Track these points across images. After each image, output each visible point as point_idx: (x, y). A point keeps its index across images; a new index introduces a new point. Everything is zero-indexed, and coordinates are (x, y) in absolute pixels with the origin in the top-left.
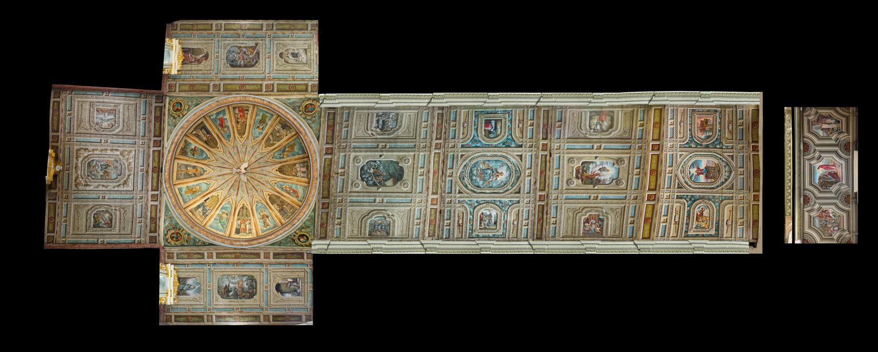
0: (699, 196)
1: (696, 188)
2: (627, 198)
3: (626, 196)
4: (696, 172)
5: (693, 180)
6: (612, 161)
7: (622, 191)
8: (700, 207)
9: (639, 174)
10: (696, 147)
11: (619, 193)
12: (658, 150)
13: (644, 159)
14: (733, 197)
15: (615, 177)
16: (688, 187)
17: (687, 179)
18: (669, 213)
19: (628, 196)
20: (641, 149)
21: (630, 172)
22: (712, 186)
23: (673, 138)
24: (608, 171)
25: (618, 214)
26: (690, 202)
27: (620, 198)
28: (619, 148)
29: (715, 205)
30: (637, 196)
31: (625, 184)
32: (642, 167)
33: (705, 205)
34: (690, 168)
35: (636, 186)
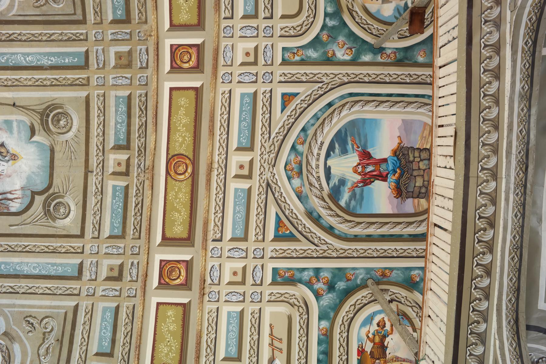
0: (368, 270)
1: (356, 239)
2: (86, 275)
3: (81, 265)
4: (355, 171)
5: (342, 203)
6: (26, 119)
7: (67, 244)
9: (127, 173)
10: (354, 62)
11: (55, 252)
12: (198, 68)
13: (144, 110)
15: (40, 184)
17: (316, 203)
18: (246, 347)
19: (87, 264)
20: (129, 65)
21: (94, 162)
23: (256, 16)
24: (14, 157)
25: (51, 339)
26: (328, 299)
27: (60, 271)
28: (45, 62)
30: (121, 266)
31: (75, 212)
32: (136, 143)
34: (328, 155)
35: (118, 223)
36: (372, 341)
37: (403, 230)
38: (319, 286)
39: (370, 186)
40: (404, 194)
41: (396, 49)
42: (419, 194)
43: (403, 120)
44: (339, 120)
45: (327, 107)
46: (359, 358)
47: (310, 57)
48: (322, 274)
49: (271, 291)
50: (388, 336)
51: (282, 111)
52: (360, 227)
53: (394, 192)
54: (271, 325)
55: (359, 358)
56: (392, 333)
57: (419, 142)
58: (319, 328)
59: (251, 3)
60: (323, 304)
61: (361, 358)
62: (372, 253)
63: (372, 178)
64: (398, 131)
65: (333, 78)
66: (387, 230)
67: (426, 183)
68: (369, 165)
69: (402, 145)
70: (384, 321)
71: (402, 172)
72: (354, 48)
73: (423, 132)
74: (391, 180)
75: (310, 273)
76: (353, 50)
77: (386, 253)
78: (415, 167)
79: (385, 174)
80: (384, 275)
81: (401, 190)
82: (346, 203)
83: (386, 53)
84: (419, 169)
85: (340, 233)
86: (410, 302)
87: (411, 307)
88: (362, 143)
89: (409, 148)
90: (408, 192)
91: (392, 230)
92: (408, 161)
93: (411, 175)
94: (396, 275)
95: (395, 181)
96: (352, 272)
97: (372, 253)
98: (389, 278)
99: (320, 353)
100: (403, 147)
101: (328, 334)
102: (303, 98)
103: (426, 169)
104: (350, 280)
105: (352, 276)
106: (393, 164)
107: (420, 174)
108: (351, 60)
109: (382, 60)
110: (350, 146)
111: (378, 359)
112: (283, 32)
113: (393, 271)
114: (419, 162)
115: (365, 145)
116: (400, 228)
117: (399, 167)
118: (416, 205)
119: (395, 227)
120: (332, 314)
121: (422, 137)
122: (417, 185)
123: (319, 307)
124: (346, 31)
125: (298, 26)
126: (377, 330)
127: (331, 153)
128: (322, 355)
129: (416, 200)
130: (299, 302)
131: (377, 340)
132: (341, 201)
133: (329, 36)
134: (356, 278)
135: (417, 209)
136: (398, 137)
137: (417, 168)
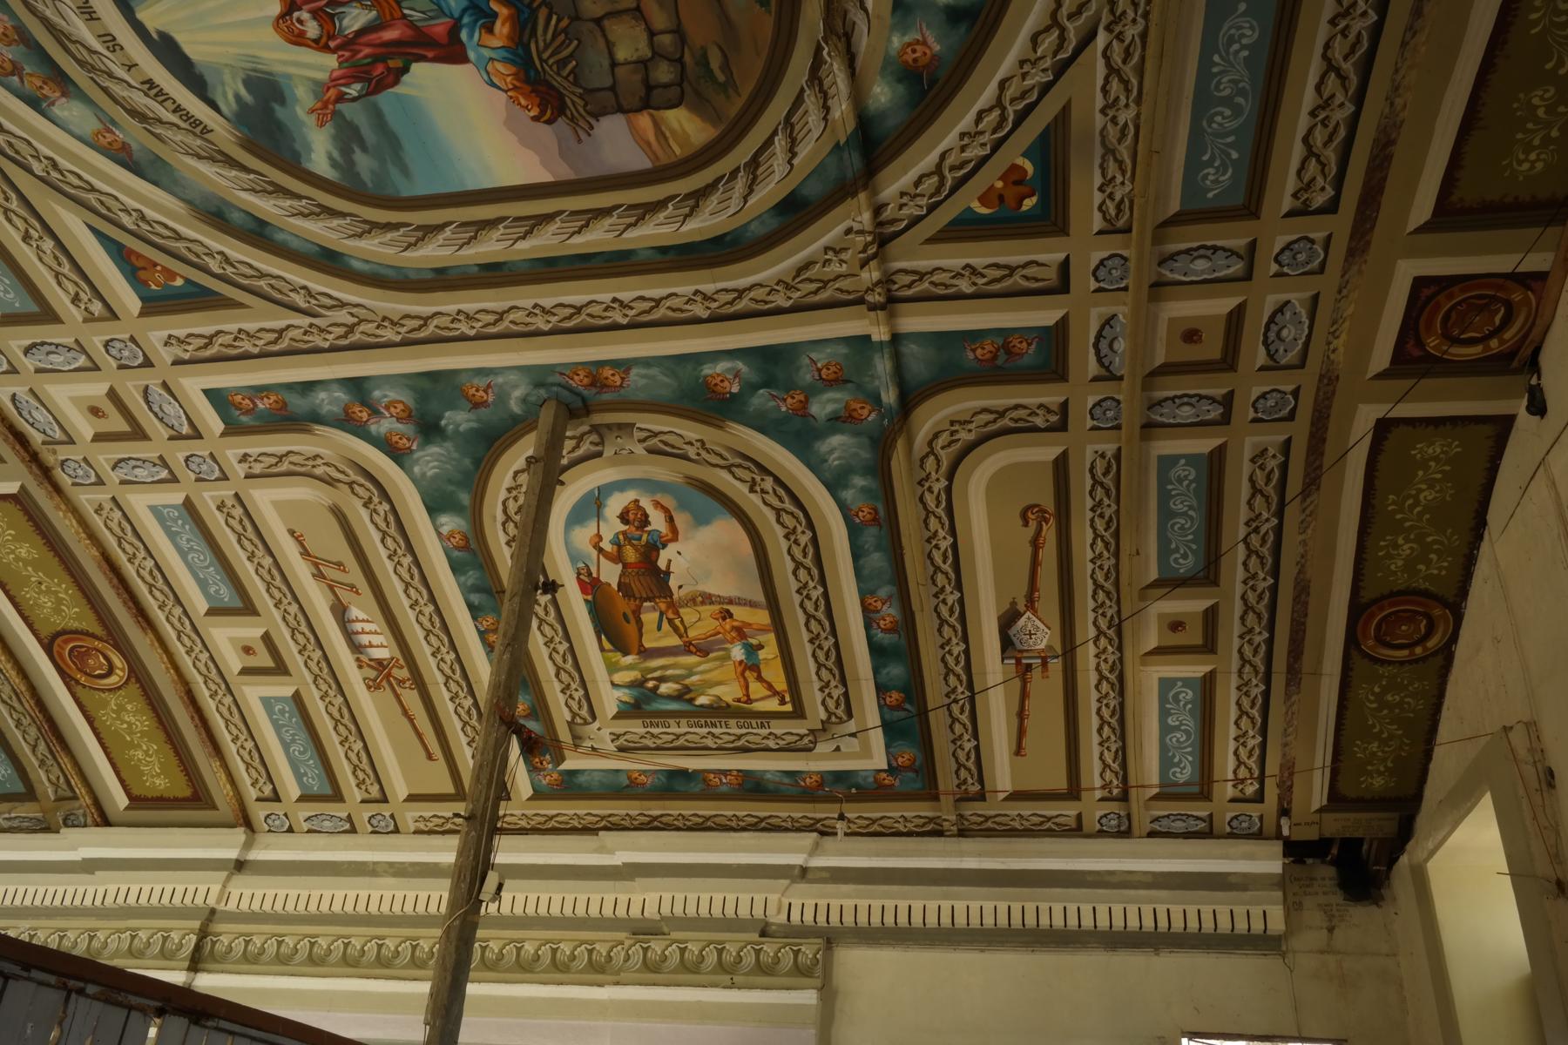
8: (592, 505)
14: (1056, 338)
16: (318, 283)
22: (705, 224)
29: (815, 466)
33: (663, 471)
36: (617, 558)
37: (624, 235)
38: (385, 426)
39: (398, 89)
40: (573, 99)
46: (590, 598)
48: (377, 394)
49: (243, 451)
50: (664, 546)
52: (441, 242)
53: (523, 102)
54: (292, 532)
55: (590, 598)
56: (675, 538)
58: (439, 534)
60: (424, 475)
61: (594, 598)
62: (529, 320)
63: (391, 56)
66: (556, 240)
67: (666, 40)
70: (639, 508)
71: (519, 11)
74: (487, 53)
75: (336, 394)
77: (583, 316)
79: (439, 27)
80: (597, 382)
81: (551, 87)
82: (334, 164)
85: (376, 266)
86: (721, 456)
87: (729, 468)
91: (577, 240)
93: (576, 18)
94: (642, 382)
96: (481, 382)
97: (529, 320)
98: (622, 391)
99: (466, 591)
101: (473, 545)
104: (484, 404)
105: (485, 391)
111: (648, 599)
113: (627, 371)
116: (607, 228)
118: (652, 138)
119: (587, 225)
120: (465, 498)
122: (622, 54)
123: (414, 480)
126: (624, 533)
128: (477, 595)
129: (644, 121)
130: (343, 472)
131: (631, 555)
132: (310, 160)
134: (502, 398)
135: (660, 153)
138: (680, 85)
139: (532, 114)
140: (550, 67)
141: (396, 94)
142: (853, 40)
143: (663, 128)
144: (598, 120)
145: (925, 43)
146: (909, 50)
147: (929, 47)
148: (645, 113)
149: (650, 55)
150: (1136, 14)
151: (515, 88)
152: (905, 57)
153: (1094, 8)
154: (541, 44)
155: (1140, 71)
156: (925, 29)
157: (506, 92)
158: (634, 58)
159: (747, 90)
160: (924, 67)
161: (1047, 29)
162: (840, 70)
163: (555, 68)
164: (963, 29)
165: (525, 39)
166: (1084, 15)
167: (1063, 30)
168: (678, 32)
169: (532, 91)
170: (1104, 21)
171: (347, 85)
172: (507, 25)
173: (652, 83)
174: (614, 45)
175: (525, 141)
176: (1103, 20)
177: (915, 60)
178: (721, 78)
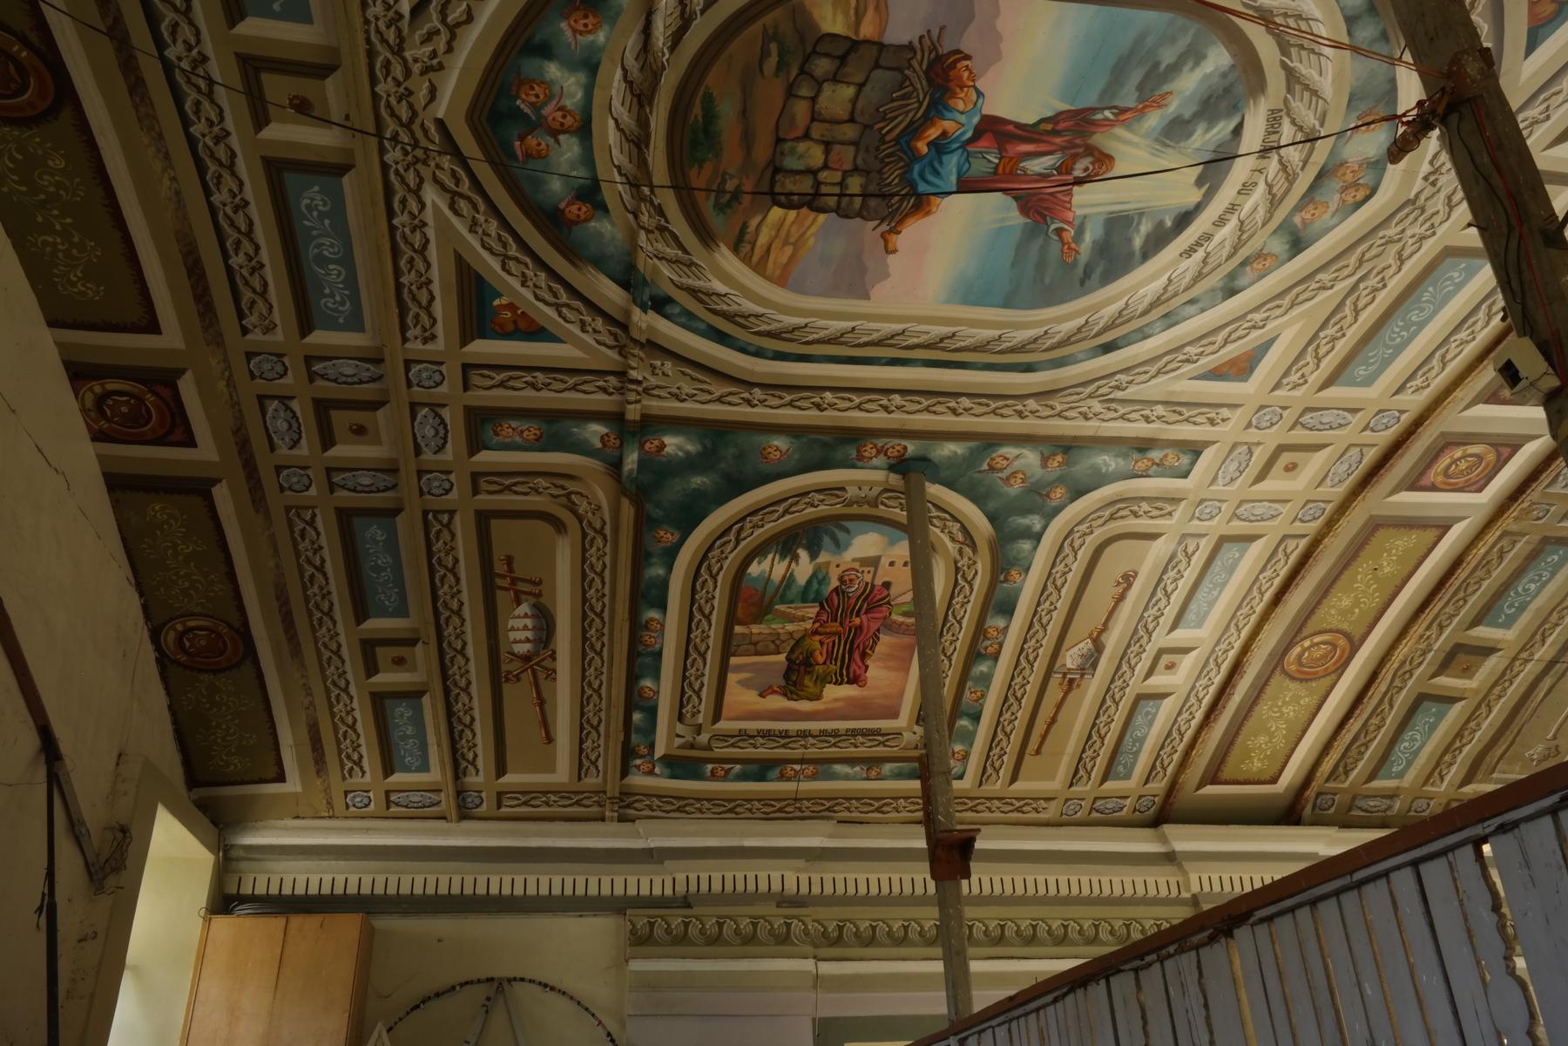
10: (991, 441)
34: (1184, 219)
39: (1065, 107)
40: (919, 65)
41: (854, 467)
42: (848, 53)
43: (867, 297)
44: (1096, 308)
45: (1120, 345)
47: (1116, 456)
51: (1271, 342)
53: (966, 74)
57: (813, 229)
59: (1223, 564)
63: (1048, 133)
64: (890, 270)
65: (1071, 408)
67: (805, 91)
68: (1039, 174)
69: (884, 227)
71: (908, 143)
72: (980, 472)
73: (791, 259)
74: (962, 119)
76: (985, 467)
78: (846, 156)
81: (929, 80)
83: (889, 458)
84: (827, 145)
88: (1040, 241)
89: (859, 215)
90: (899, 70)
92: (874, 175)
95: (948, 115)
100: (882, 220)
102: (1188, 367)
103: (797, 139)
106: (936, 173)
107: (827, 126)
108: (1000, 445)
109: (904, 442)
110: (1088, 237)
112: (1169, 508)
114: (825, 167)
115: (1029, 235)
117: (916, 157)
121: (798, 245)
122: (850, 91)
124: (991, 505)
125: (1122, 517)
127: (1169, 223)
129: (867, 30)
133: (1048, 496)
136: (895, 251)
137: (837, 148)
138: (814, 51)
139: (968, 62)
140: (918, 96)
141: (1072, 105)
142: (640, 46)
143: (853, 18)
144: (910, 43)
145: (575, 31)
146: (590, 27)
147: (569, 24)
148: (861, 37)
149: (825, 84)
150: (376, 25)
151: (962, 88)
152: (595, 21)
153: (417, 37)
154: (911, 115)
155: (371, 54)
156: (573, 43)
157: (974, 87)
158: (840, 85)
159: (756, 28)
160: (578, 9)
161: (458, 25)
162: (658, 39)
163: (915, 94)
164: (537, 38)
165: (922, 119)
166: (425, 31)
167: (444, 21)
168: (790, 93)
169: (952, 81)
170: (405, 24)
171: (1107, 119)
172: (926, 134)
173: (837, 62)
174: (850, 101)
175: (994, 39)
176: (406, 26)
177: (586, 17)
178: (774, 47)
